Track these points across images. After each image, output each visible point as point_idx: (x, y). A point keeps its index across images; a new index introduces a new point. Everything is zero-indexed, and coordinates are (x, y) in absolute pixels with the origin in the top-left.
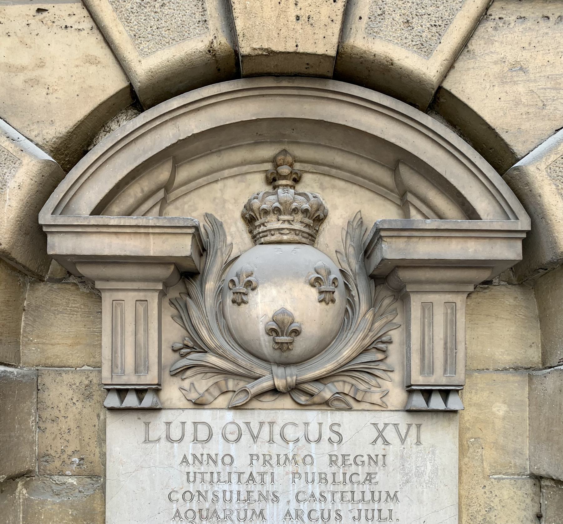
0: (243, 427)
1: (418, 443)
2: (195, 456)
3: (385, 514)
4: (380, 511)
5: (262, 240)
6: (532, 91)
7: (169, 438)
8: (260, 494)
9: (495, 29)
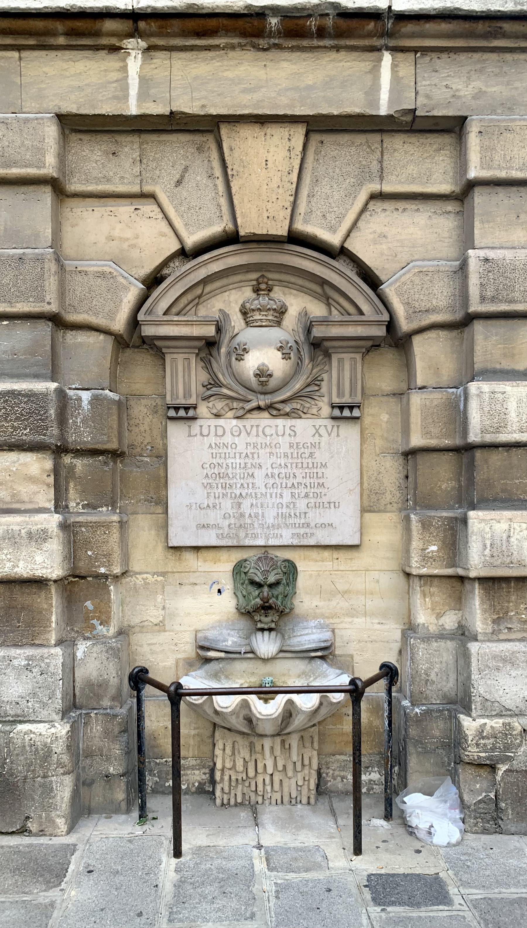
0: (242, 428)
1: (338, 435)
2: (216, 444)
3: (320, 475)
4: (317, 473)
5: (251, 325)
6: (390, 248)
7: (201, 434)
8: (252, 464)
9: (371, 215)
